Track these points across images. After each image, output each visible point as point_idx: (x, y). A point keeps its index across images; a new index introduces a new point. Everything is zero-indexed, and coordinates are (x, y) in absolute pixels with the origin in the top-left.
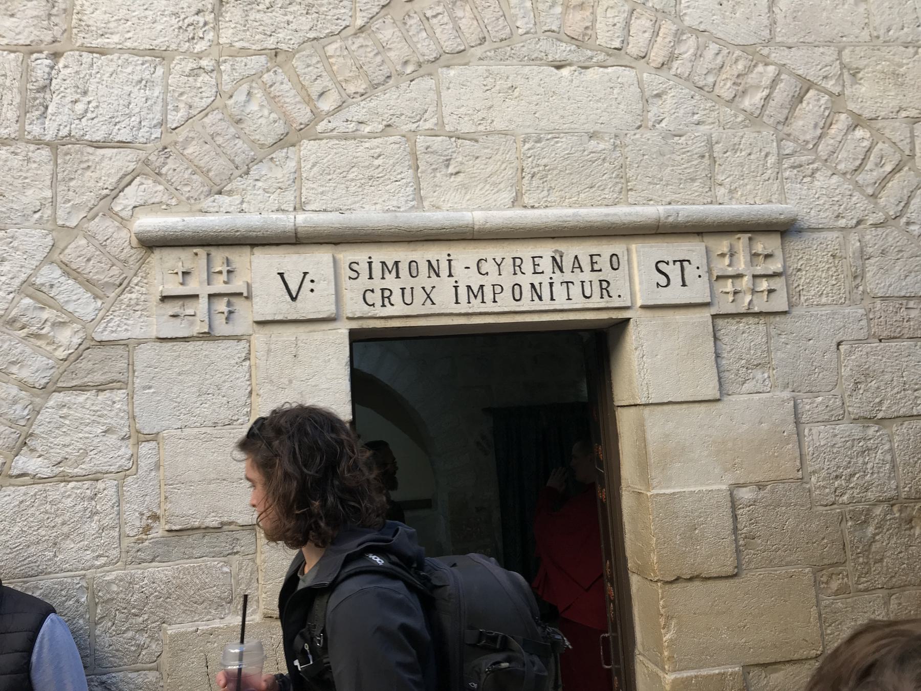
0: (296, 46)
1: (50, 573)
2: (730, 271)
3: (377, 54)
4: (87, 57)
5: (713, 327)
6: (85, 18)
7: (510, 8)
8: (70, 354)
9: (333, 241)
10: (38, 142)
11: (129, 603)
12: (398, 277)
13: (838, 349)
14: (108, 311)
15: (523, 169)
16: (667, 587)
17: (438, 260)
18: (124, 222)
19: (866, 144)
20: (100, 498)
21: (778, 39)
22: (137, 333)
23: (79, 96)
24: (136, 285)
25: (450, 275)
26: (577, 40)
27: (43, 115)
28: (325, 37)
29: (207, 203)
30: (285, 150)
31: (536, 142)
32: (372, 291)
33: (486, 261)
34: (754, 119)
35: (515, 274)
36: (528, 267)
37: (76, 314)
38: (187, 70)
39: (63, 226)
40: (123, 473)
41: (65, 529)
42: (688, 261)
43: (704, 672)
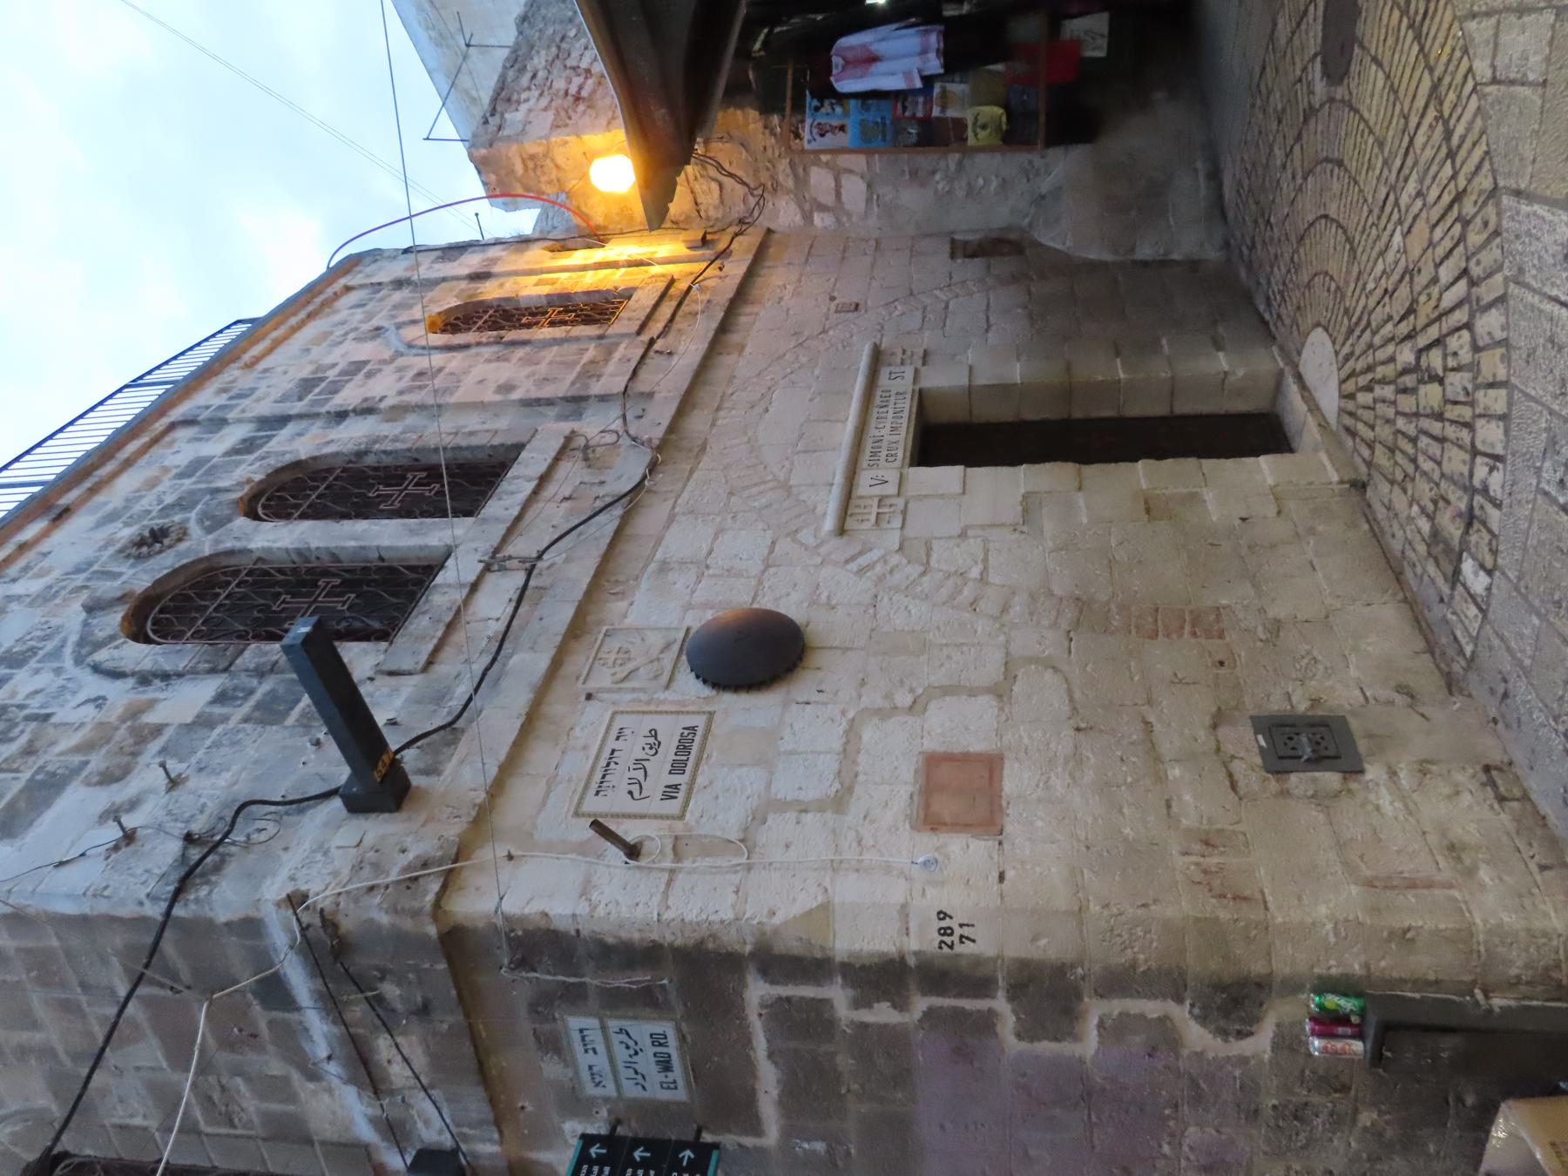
4: (713, 555)
10: (763, 572)
40: (985, 541)
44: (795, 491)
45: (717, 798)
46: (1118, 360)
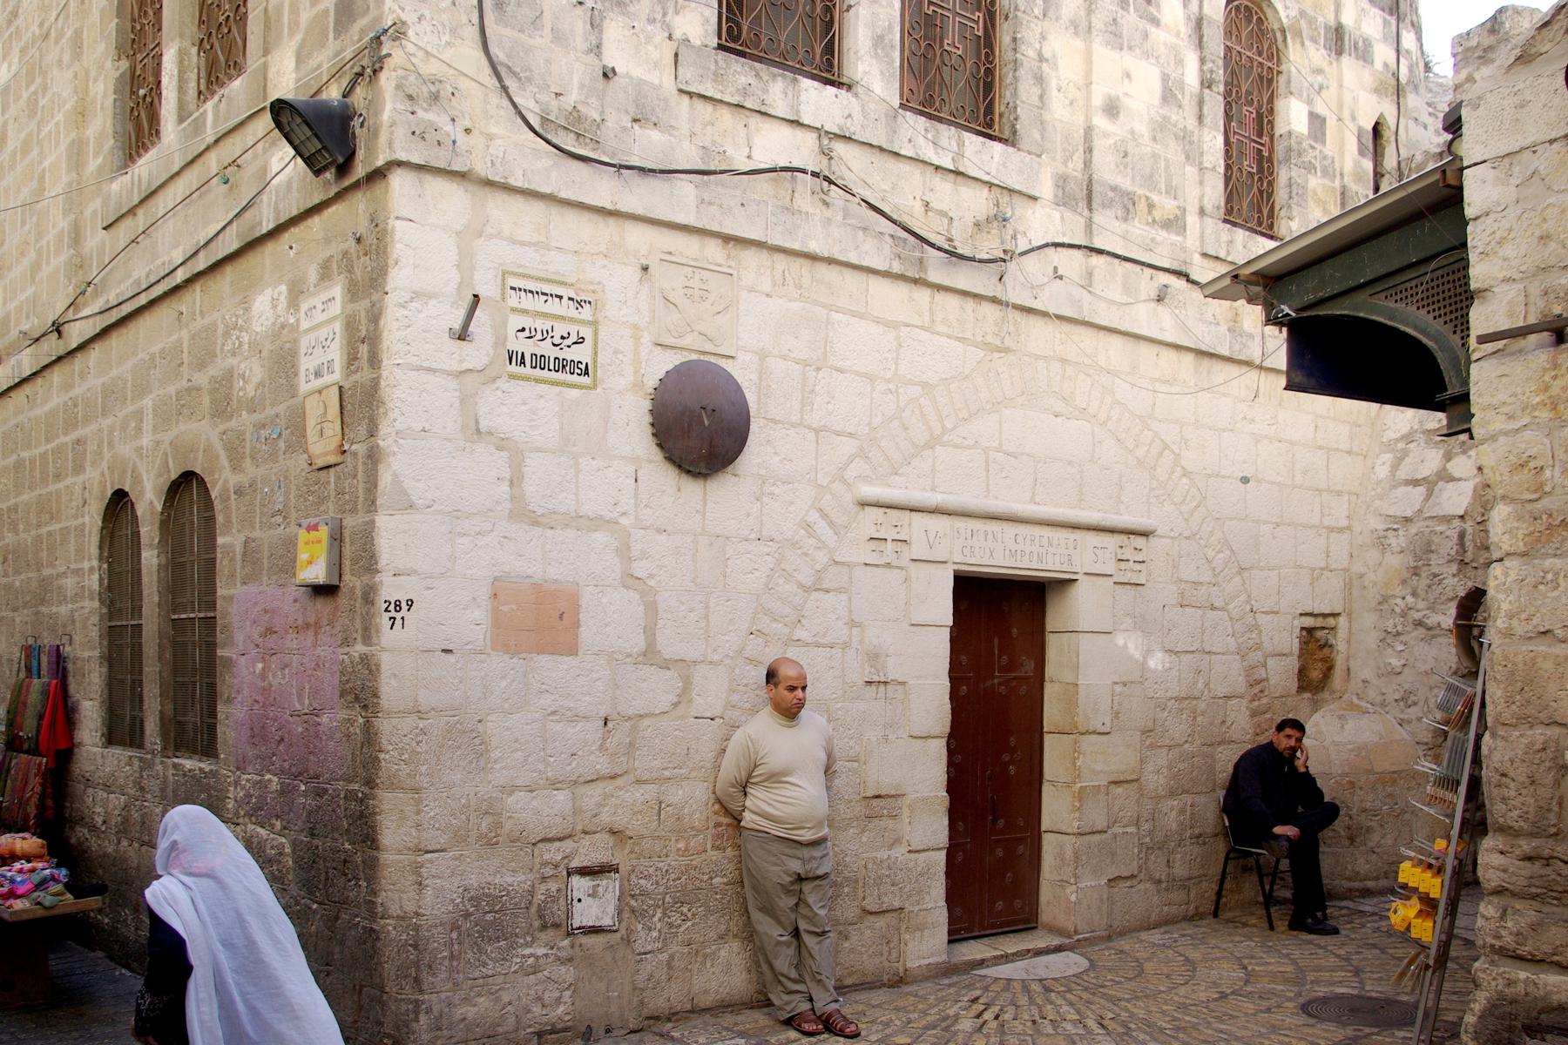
2: (1124, 557)
22: (853, 559)
27: (812, 410)
40: (845, 646)
44: (926, 453)
45: (525, 404)
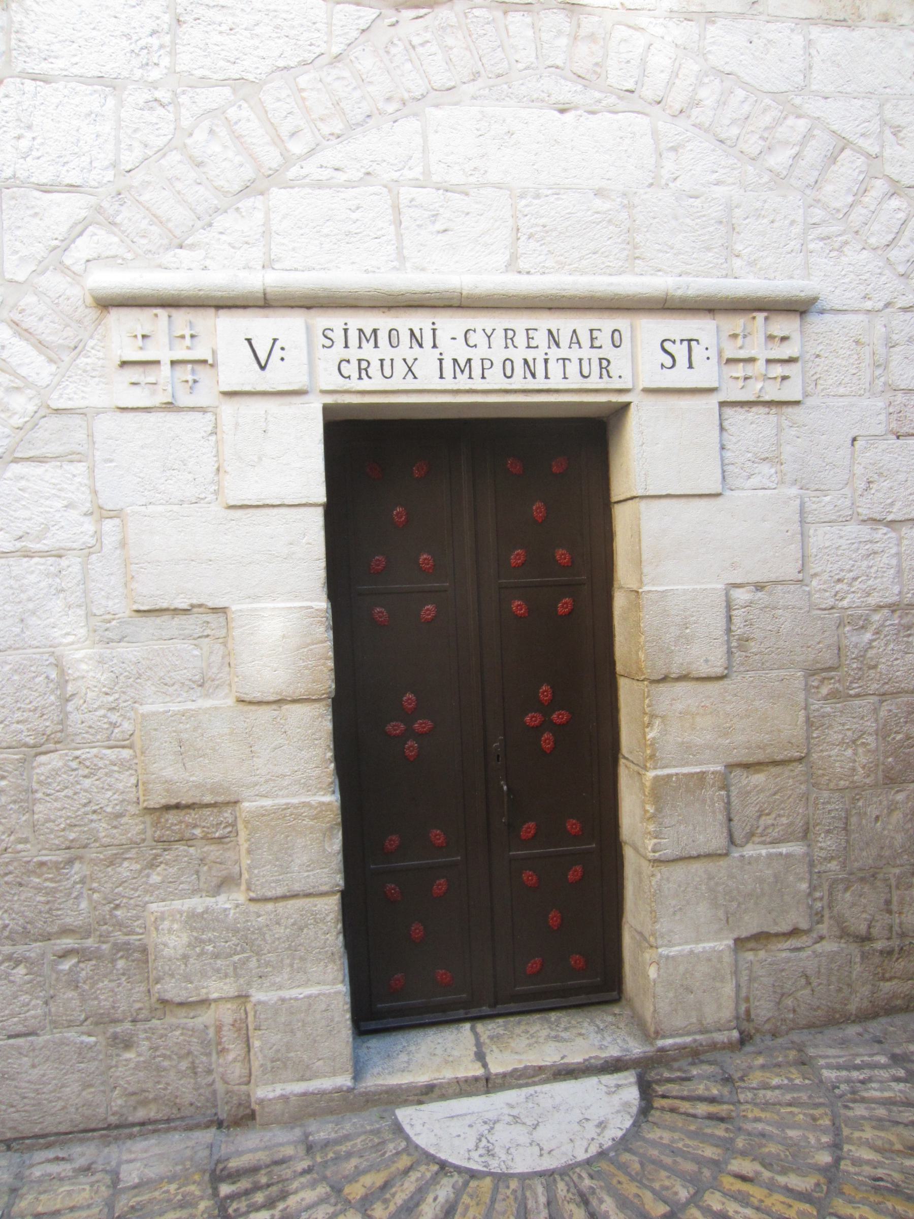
0: (264, 76)
1: (18, 649)
2: (743, 354)
3: (355, 88)
4: (30, 85)
5: (720, 415)
6: (25, 38)
7: (508, 36)
8: (26, 422)
9: (308, 303)
11: (99, 681)
12: (376, 346)
13: (853, 445)
14: (64, 376)
15: (518, 229)
16: (654, 686)
17: (421, 329)
18: (76, 277)
19: (902, 215)
20: (65, 575)
21: (814, 87)
23: (22, 131)
24: (93, 348)
25: (435, 346)
26: (583, 78)
28: (296, 66)
29: (168, 258)
30: (252, 199)
31: (534, 198)
32: (348, 361)
33: (475, 331)
34: (779, 179)
35: (507, 347)
36: (521, 340)
37: (30, 379)
38: (141, 102)
39: (11, 281)
40: (88, 551)
41: (31, 606)
42: (697, 341)
43: (685, 770)
46: (719, 768)
